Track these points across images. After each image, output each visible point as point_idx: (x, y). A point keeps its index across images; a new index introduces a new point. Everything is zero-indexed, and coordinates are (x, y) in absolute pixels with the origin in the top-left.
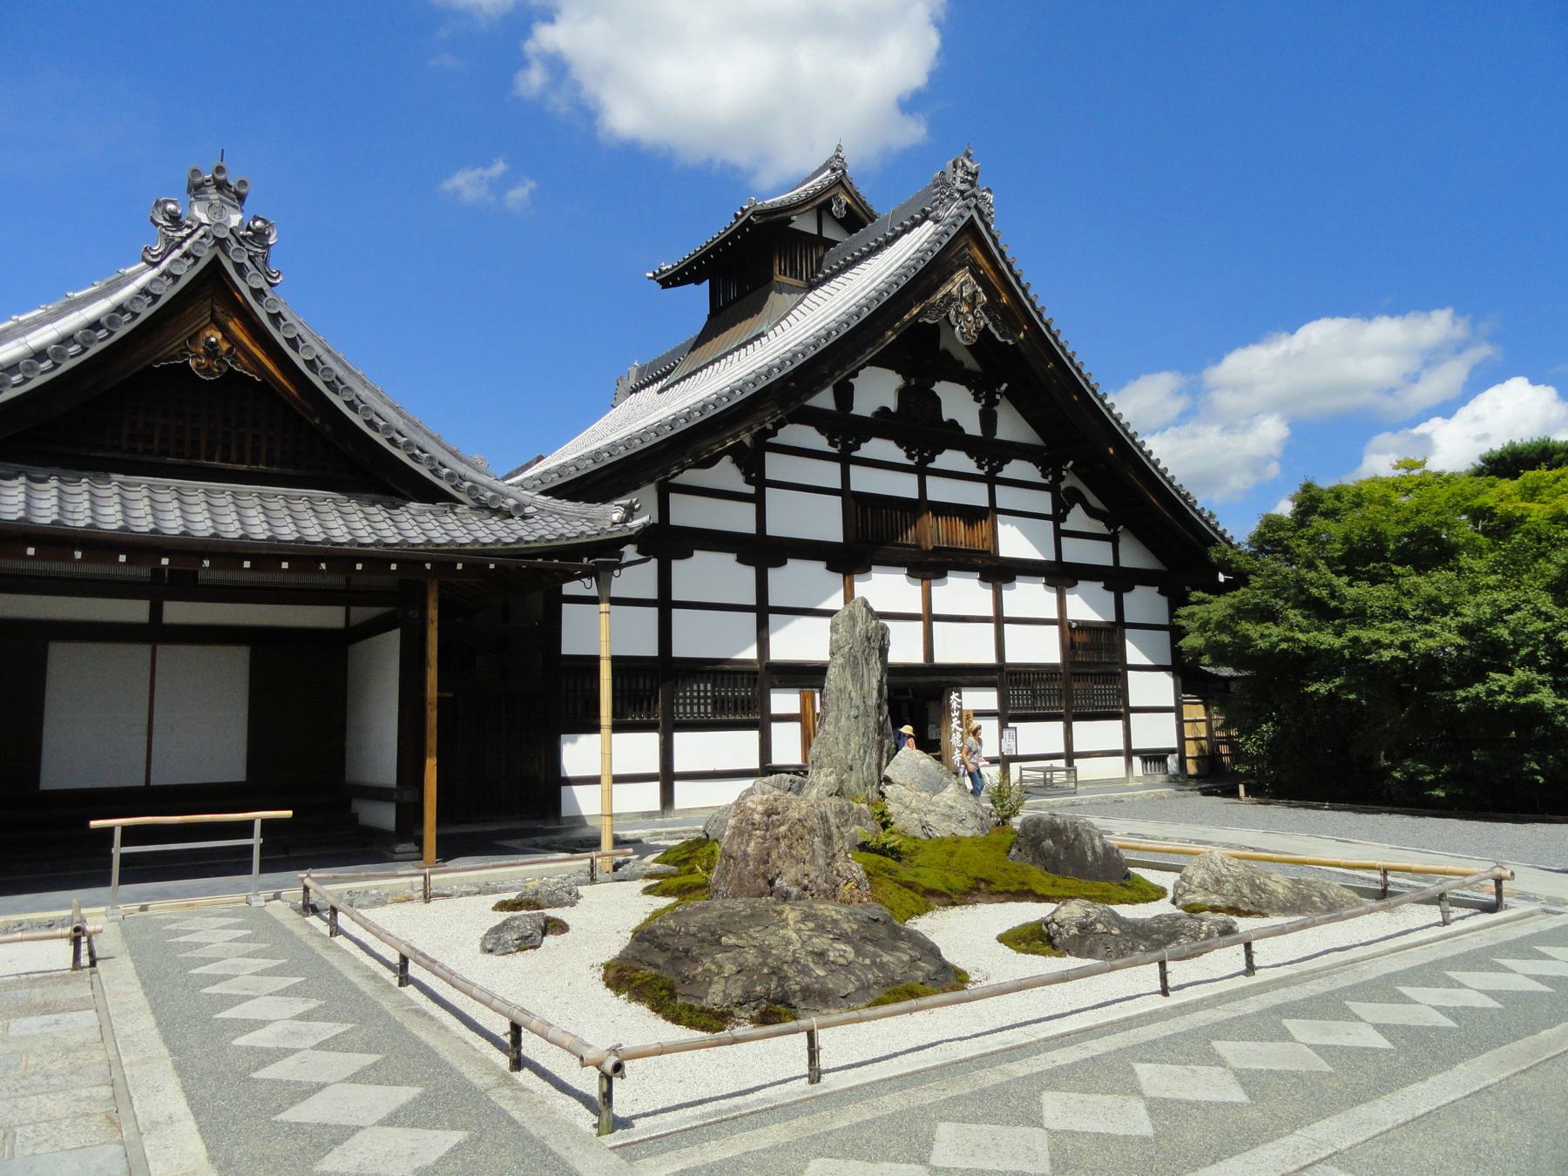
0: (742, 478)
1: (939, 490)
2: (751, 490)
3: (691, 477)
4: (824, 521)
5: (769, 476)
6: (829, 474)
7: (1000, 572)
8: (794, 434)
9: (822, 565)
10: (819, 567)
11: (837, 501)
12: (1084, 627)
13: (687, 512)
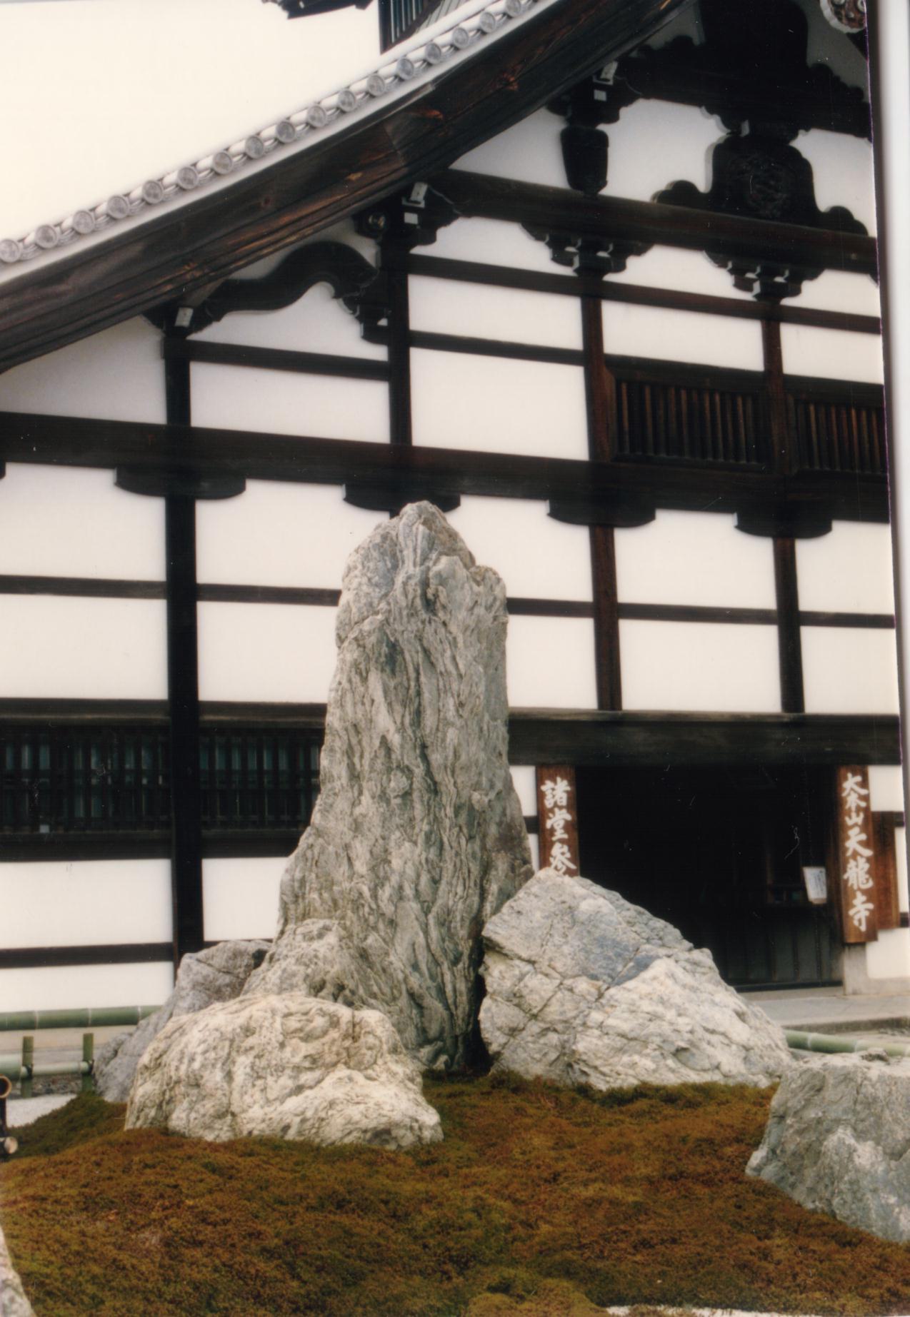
2: (379, 353)
3: (239, 328)
4: (549, 417)
6: (558, 320)
8: (468, 238)
9: (539, 510)
10: (534, 513)
11: (572, 379)
13: (229, 401)
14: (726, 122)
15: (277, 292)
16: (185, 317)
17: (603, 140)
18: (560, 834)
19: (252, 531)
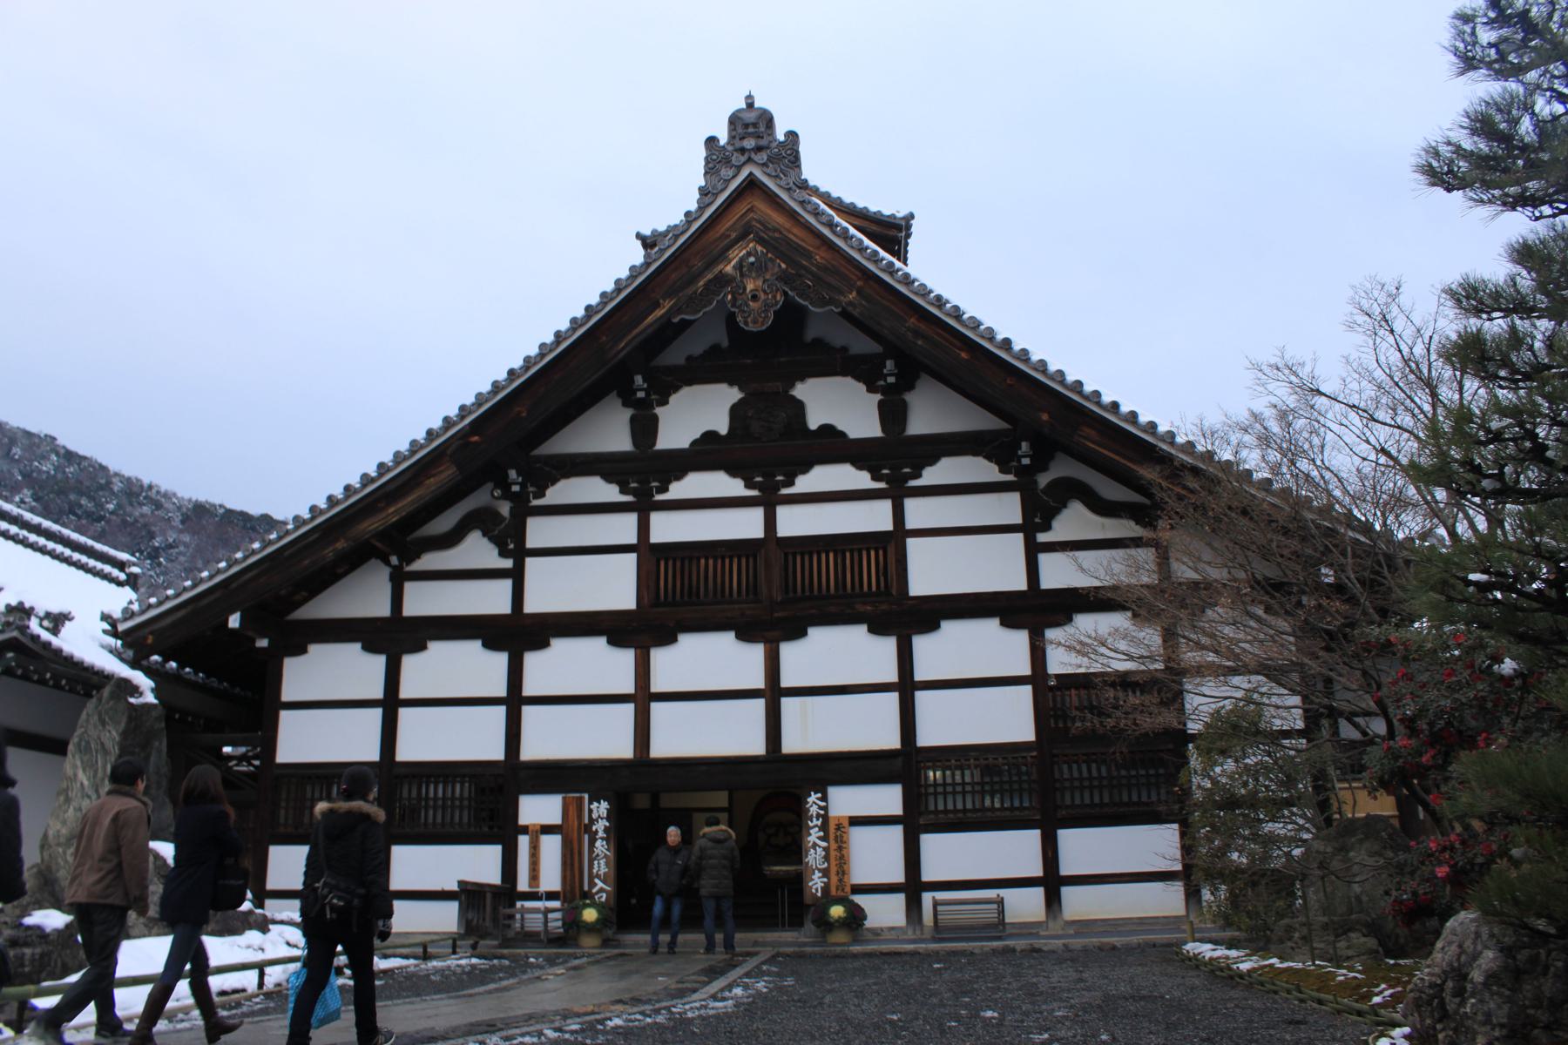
0: (496, 551)
1: (795, 522)
2: (508, 563)
4: (614, 586)
5: (531, 543)
6: (623, 528)
7: (907, 617)
9: (601, 642)
12: (1068, 681)
13: (423, 601)
14: (741, 389)
15: (450, 540)
16: (394, 560)
17: (655, 419)
18: (601, 834)
19: (428, 670)
